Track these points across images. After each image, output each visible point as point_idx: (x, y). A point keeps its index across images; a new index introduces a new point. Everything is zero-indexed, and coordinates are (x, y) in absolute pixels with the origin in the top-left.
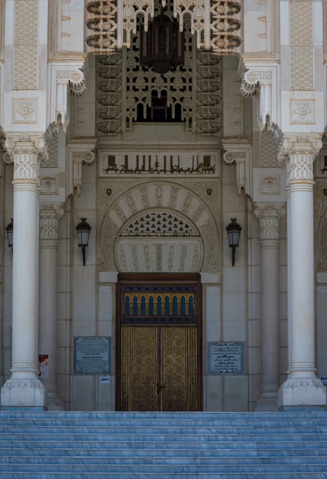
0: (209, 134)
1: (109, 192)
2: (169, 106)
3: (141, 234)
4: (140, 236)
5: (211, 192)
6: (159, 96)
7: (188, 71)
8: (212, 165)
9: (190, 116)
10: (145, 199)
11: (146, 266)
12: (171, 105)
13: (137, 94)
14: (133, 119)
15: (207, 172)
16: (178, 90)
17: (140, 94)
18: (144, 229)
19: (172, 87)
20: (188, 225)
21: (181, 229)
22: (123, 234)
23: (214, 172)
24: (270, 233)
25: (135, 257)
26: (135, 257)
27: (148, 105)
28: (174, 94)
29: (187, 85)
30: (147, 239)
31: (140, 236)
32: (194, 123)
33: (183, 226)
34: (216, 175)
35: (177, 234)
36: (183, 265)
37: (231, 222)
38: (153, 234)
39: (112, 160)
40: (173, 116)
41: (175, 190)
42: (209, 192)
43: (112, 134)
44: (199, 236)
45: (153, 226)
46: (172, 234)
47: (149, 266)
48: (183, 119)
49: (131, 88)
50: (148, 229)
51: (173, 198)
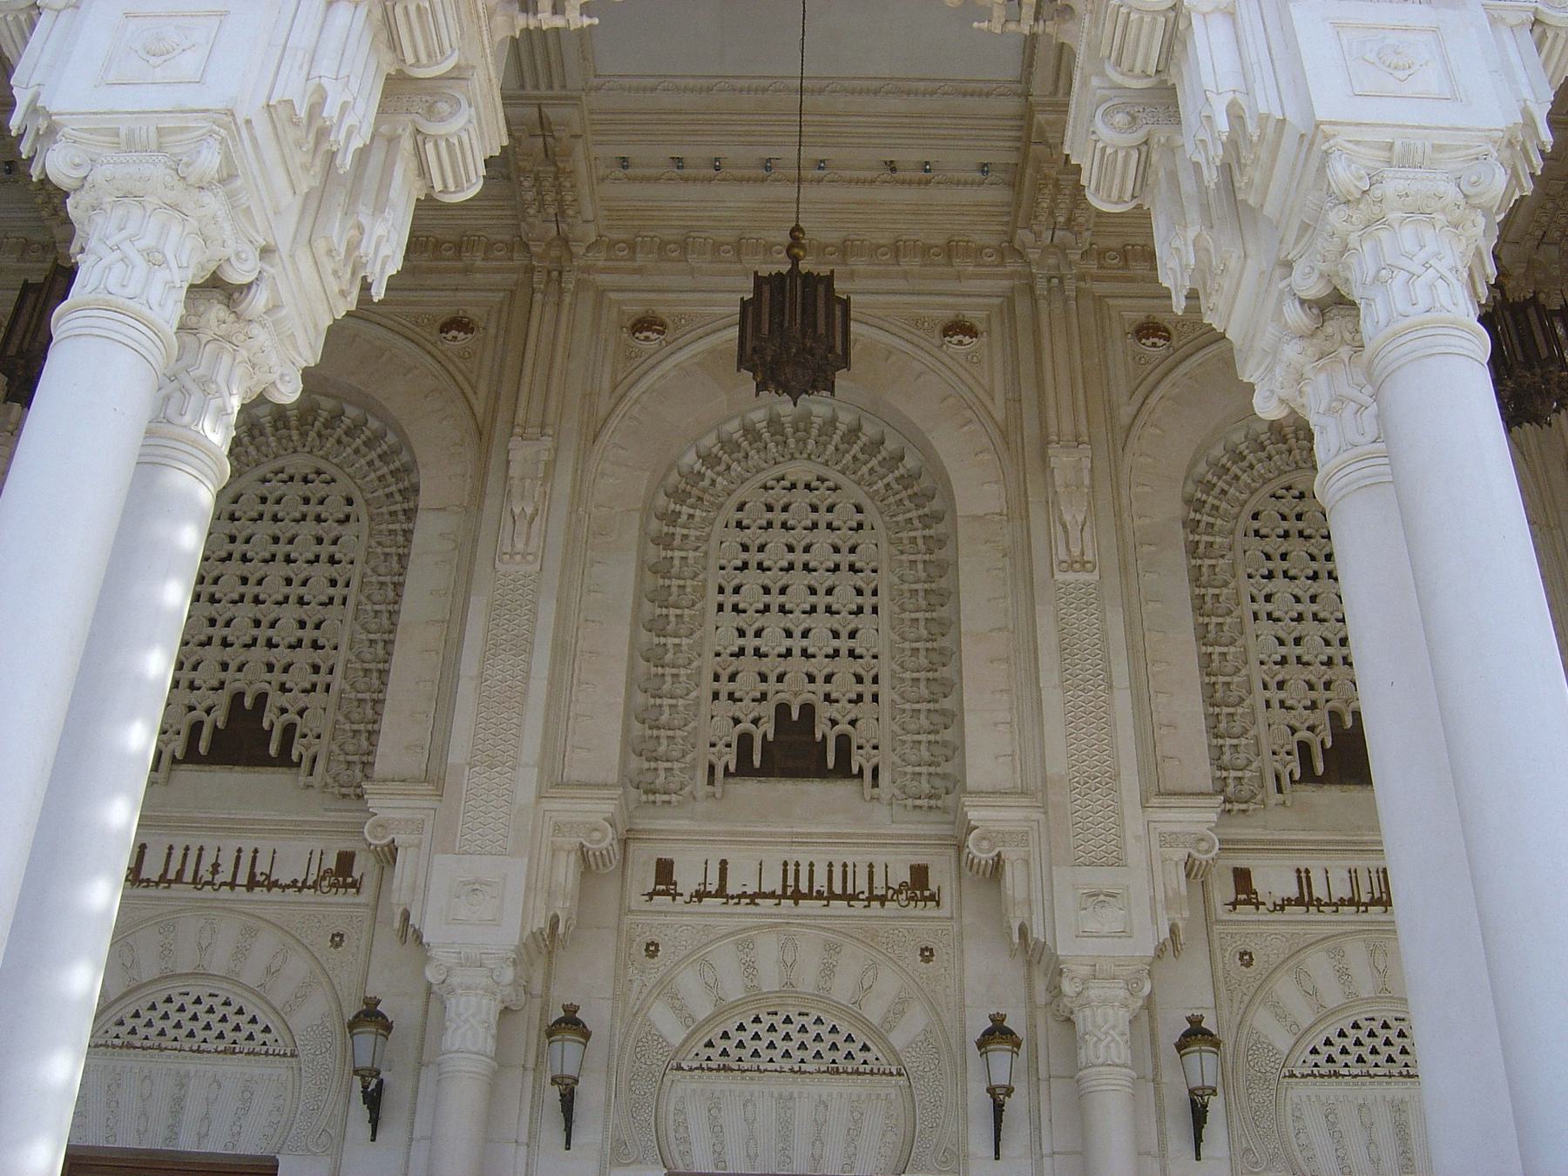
0: (923, 802)
1: (652, 949)
2: (819, 736)
3: (735, 1066)
4: (732, 1070)
5: (932, 954)
6: (795, 716)
7: (868, 658)
8: (933, 887)
9: (874, 761)
10: (750, 968)
11: (748, 1156)
12: (824, 737)
13: (736, 709)
14: (726, 768)
15: (921, 904)
16: (845, 613)
17: (747, 710)
18: (746, 1054)
19: (827, 697)
20: (868, 1043)
21: (849, 1055)
22: (684, 1065)
23: (938, 904)
24: (1108, 1046)
25: (716, 1129)
26: (716, 1129)
27: (765, 735)
28: (832, 711)
29: (867, 689)
30: (751, 1079)
31: (732, 1070)
32: (884, 777)
33: (854, 1048)
34: (945, 911)
35: (837, 1068)
36: (855, 1155)
37: (990, 1024)
38: (771, 1066)
39: (664, 870)
40: (831, 764)
41: (832, 948)
42: (927, 954)
43: (666, 798)
44: (900, 1074)
45: (772, 1045)
46: (823, 1068)
47: (756, 1155)
48: (855, 770)
49: (723, 696)
50: (756, 1054)
51: (828, 971)
